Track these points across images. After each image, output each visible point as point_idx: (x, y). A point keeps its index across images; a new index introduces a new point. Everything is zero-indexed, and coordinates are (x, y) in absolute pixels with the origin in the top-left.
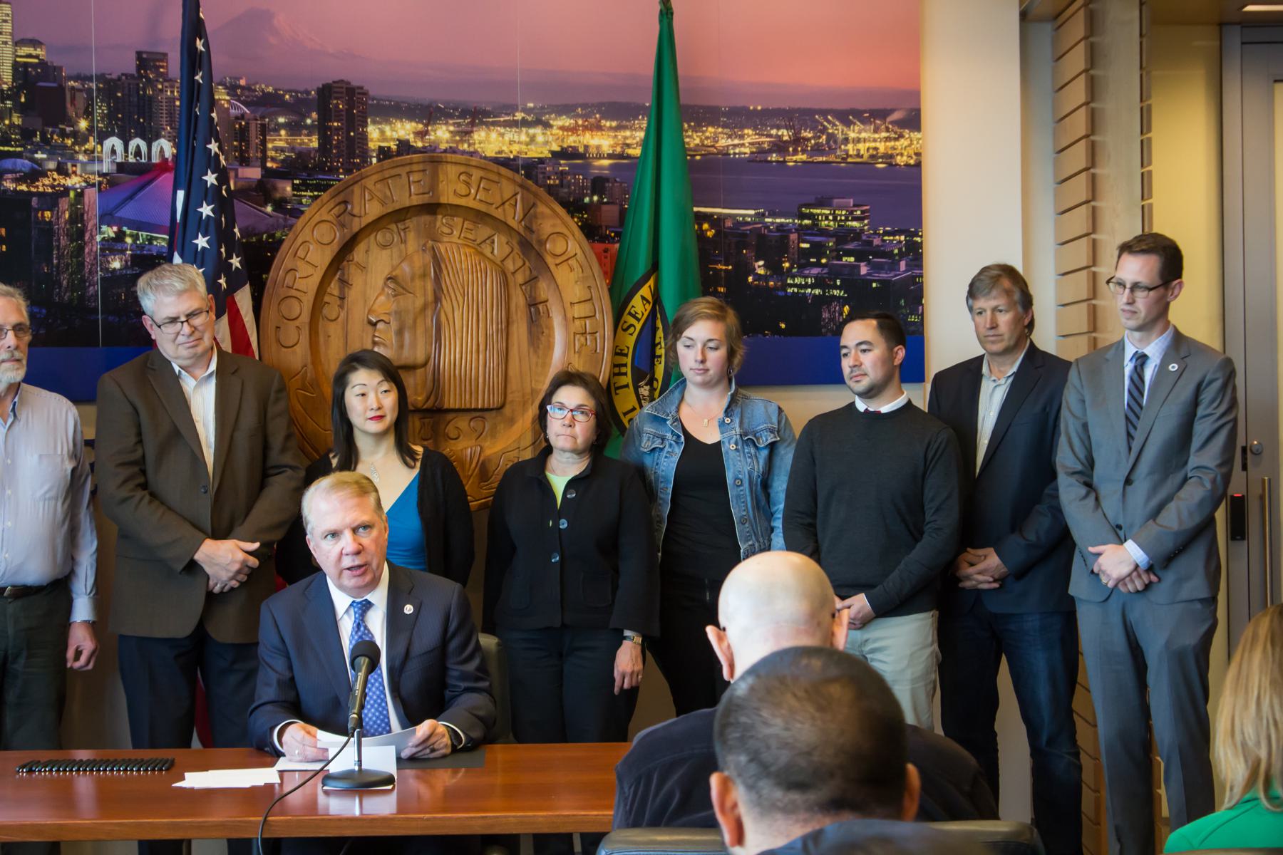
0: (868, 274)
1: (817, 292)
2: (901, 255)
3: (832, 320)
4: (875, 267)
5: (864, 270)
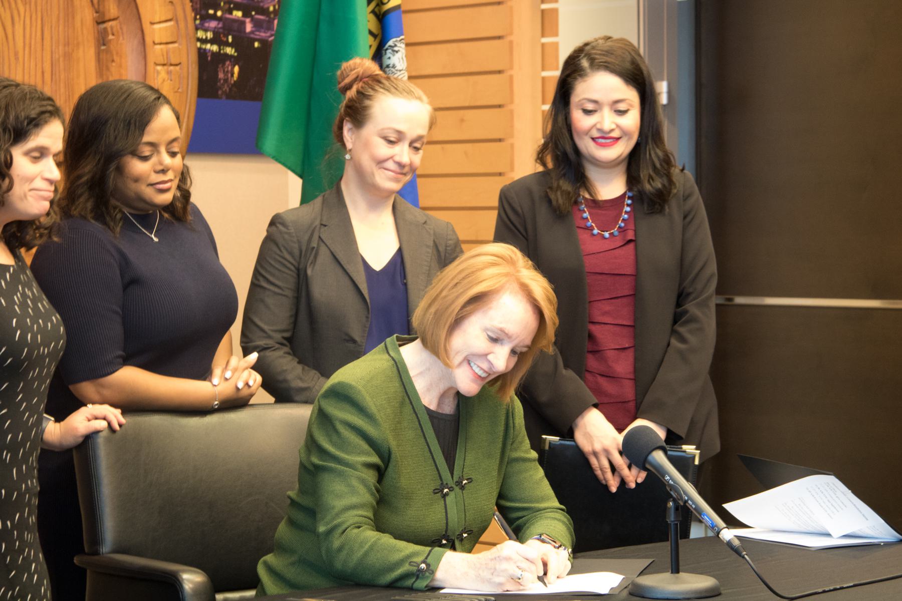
0: (252, 32)
1: (215, 48)
2: (276, 12)
3: (226, 80)
4: (257, 25)
5: (249, 27)
